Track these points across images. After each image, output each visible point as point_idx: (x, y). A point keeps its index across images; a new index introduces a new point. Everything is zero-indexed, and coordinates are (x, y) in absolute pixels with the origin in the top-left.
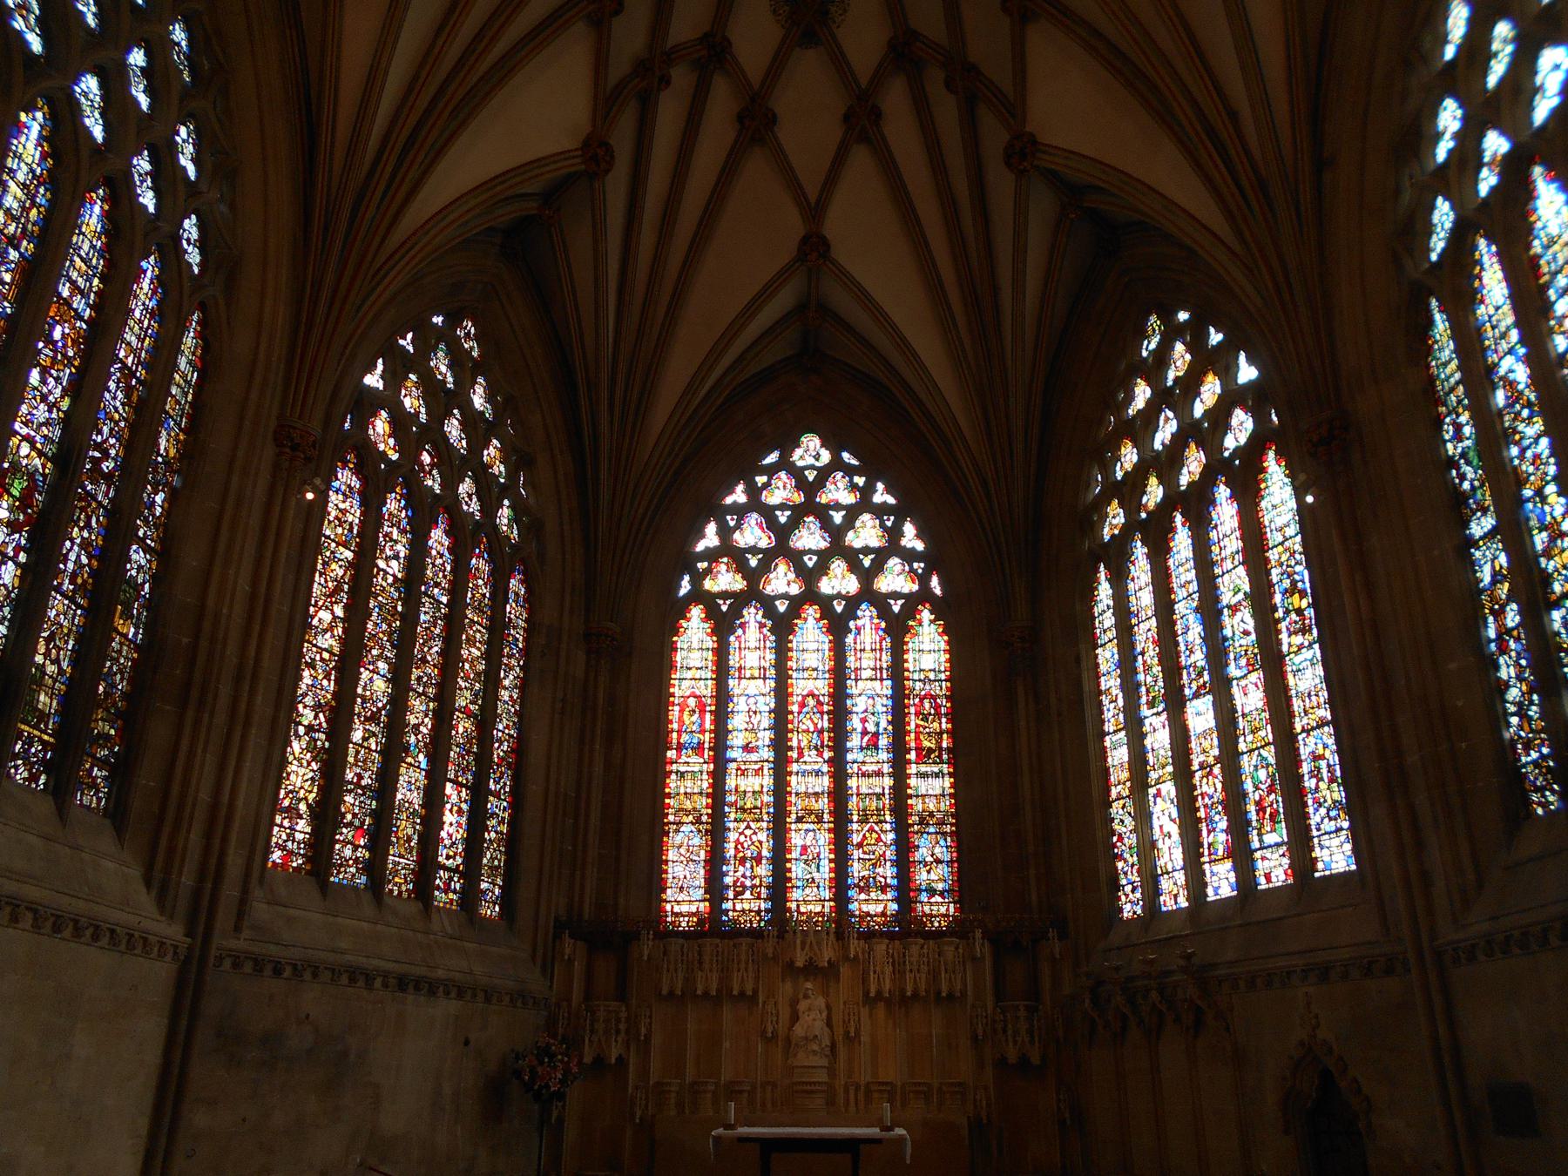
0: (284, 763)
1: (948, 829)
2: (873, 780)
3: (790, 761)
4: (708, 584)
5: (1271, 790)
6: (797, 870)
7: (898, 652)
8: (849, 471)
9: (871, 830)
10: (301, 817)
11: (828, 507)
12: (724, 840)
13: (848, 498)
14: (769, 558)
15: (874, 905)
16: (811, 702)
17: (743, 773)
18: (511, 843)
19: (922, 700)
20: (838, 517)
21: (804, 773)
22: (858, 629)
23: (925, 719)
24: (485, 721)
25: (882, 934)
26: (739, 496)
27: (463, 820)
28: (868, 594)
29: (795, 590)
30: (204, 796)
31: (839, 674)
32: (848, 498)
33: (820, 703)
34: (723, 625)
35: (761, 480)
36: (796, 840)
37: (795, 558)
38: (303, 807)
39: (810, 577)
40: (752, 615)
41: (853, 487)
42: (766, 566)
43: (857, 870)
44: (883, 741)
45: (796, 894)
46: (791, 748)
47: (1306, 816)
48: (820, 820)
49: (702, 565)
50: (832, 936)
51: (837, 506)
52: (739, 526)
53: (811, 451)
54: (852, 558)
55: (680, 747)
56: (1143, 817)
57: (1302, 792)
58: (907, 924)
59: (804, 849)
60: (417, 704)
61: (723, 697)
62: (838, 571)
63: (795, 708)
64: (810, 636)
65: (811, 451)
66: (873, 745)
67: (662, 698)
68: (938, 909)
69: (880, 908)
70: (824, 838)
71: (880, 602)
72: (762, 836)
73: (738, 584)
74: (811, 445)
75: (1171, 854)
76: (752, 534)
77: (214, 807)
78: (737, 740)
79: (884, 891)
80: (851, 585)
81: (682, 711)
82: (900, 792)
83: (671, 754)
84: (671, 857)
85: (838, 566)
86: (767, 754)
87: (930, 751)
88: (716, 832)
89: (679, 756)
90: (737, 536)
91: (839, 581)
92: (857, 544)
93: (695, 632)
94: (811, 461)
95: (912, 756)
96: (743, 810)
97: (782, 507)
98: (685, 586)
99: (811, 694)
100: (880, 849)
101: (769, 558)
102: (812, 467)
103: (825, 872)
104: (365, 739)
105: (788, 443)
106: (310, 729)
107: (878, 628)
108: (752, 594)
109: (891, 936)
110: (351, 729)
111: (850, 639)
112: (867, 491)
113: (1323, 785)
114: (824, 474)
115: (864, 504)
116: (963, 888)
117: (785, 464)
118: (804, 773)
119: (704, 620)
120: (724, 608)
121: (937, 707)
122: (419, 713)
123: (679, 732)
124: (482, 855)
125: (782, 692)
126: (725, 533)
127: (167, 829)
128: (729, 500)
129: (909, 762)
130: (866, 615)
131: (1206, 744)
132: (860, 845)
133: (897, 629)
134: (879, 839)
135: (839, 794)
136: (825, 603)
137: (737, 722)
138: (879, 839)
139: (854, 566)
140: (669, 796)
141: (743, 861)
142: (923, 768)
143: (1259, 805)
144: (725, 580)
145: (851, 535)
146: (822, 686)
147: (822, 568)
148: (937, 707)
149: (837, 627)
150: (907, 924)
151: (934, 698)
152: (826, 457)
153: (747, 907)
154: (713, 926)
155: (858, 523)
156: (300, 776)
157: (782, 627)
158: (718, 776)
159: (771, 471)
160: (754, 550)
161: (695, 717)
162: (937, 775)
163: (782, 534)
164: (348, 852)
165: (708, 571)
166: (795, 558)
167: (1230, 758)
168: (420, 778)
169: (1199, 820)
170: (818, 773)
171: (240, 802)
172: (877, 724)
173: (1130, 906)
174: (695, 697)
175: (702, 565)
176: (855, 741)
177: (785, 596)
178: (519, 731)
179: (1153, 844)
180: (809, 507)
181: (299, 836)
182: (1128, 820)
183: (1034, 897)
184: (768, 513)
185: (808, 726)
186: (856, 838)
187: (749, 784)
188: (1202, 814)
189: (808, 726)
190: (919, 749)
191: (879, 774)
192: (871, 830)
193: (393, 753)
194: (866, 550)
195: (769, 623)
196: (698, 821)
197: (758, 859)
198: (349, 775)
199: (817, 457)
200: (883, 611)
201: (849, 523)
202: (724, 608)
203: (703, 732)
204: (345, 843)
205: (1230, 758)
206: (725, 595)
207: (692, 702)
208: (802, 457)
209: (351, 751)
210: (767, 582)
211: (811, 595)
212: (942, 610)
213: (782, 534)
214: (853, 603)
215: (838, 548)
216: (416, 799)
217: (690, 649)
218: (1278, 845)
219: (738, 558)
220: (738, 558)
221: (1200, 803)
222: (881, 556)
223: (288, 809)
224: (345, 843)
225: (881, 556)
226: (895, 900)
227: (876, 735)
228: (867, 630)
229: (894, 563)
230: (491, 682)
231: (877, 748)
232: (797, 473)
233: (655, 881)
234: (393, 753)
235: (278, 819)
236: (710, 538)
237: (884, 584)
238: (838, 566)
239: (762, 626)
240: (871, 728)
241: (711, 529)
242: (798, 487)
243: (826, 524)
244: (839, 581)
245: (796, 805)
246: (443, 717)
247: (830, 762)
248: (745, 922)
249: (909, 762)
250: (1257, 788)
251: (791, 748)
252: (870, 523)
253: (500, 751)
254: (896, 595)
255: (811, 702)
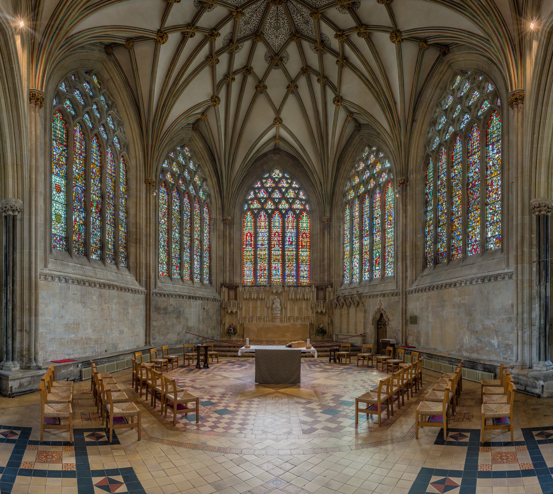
0: (159, 254)
1: (308, 263)
2: (291, 252)
3: (272, 248)
4: (251, 206)
5: (379, 258)
6: (274, 272)
7: (298, 223)
8: (287, 179)
9: (290, 263)
10: (164, 264)
11: (281, 188)
12: (257, 265)
13: (286, 185)
14: (266, 200)
15: (290, 280)
16: (277, 234)
17: (261, 250)
18: (210, 268)
19: (303, 234)
20: (284, 190)
21: (275, 250)
22: (288, 217)
23: (304, 238)
24: (201, 242)
25: (292, 286)
26: (259, 185)
27: (199, 263)
28: (290, 209)
29: (273, 207)
30: (144, 262)
31: (283, 228)
32: (286, 185)
33: (279, 234)
34: (256, 216)
35: (264, 181)
36: (273, 265)
37: (273, 200)
38: (164, 262)
39: (276, 204)
40: (262, 213)
41: (287, 183)
42: (266, 202)
43: (287, 272)
44: (294, 243)
45: (273, 277)
46: (272, 245)
47: (385, 264)
48: (279, 261)
49: (250, 202)
50: (281, 287)
51: (283, 187)
52: (259, 192)
53: (277, 174)
54: (287, 200)
55: (246, 245)
56: (351, 262)
57: (385, 259)
58: (298, 285)
59: (275, 267)
60: (186, 238)
61: (256, 233)
62: (284, 203)
63: (273, 235)
64: (277, 218)
65: (277, 174)
66: (291, 244)
67: (242, 234)
68: (305, 281)
69: (292, 281)
70: (280, 265)
71: (294, 211)
72: (266, 265)
73: (259, 206)
74: (277, 172)
75: (357, 270)
76: (262, 194)
77: (146, 264)
78: (260, 243)
79: (293, 277)
80: (287, 206)
81: (246, 237)
82: (297, 255)
83: (245, 246)
84: (245, 269)
85: (284, 202)
86: (266, 246)
87: (304, 246)
88: (255, 264)
89: (246, 247)
90: (259, 195)
91: (284, 205)
92: (288, 197)
93: (249, 217)
94: (277, 176)
95: (300, 247)
96: (261, 259)
97: (270, 187)
98: (246, 207)
99: (277, 232)
100: (292, 268)
101: (266, 200)
102: (277, 178)
103: (280, 273)
104: (175, 247)
105: (271, 171)
106: (163, 246)
107: (293, 217)
108: (263, 209)
109: (294, 287)
110: (172, 245)
111: (286, 219)
112: (291, 184)
113: (389, 258)
114: (280, 179)
115: (290, 187)
116: (310, 276)
117: (270, 177)
118: (275, 250)
119: (251, 215)
120: (256, 212)
121: (307, 236)
122: (186, 240)
123: (246, 241)
124: (204, 270)
125: (270, 232)
126: (255, 193)
127: (138, 269)
128: (256, 186)
129: (300, 248)
130: (290, 213)
131: (367, 247)
132: (288, 267)
133: (298, 217)
134: (292, 265)
135: (283, 255)
136: (280, 211)
137: (260, 238)
138: (292, 265)
139: (287, 202)
140: (244, 256)
141: (261, 270)
142: (303, 250)
143: (376, 261)
144: (256, 205)
145: (287, 194)
146: (279, 230)
147: (280, 202)
148: (307, 236)
149: (283, 216)
150: (298, 285)
151: (306, 234)
152: (281, 175)
153: (263, 280)
154: (255, 285)
155: (289, 191)
156: (163, 256)
157: (270, 217)
158: (255, 251)
159: (266, 178)
160: (263, 198)
161: (250, 238)
162: (306, 251)
163: (270, 194)
164: (175, 271)
165: (252, 203)
166: (273, 200)
167: (371, 250)
168: (188, 254)
169: (363, 264)
170: (278, 250)
171: (151, 262)
172: (292, 239)
173: (347, 281)
174: (250, 233)
175: (250, 202)
176: (287, 243)
177: (270, 209)
178: (209, 242)
179: (353, 268)
180: (277, 187)
181: (165, 269)
182: (348, 263)
183: (326, 279)
184: (266, 189)
185: (276, 240)
186: (287, 265)
187: (263, 253)
188: (364, 262)
189: (276, 240)
190: (302, 245)
191: (292, 251)
192: (290, 263)
193: (182, 249)
194: (291, 198)
195: (267, 216)
196: (251, 261)
197: (265, 270)
198: (173, 255)
199: (278, 175)
200: (294, 213)
201: (287, 191)
202: (256, 212)
203: (251, 241)
204: (174, 269)
205: (371, 250)
206: (256, 209)
207: (249, 234)
208: (274, 175)
209: (173, 250)
210: (266, 206)
211: (277, 209)
212: (308, 213)
213: (270, 194)
214: (287, 211)
215: (284, 197)
216: (188, 259)
217: (248, 222)
218: (379, 269)
219: (259, 200)
220: (259, 200)
221: (364, 260)
222: (294, 199)
223: (162, 263)
224: (174, 269)
225: (294, 199)
226: (296, 279)
227: (292, 242)
228: (290, 217)
229: (298, 201)
230: (202, 231)
231: (292, 244)
232: (273, 179)
233: (242, 275)
234: (182, 249)
235: (160, 265)
236: (252, 195)
237: (295, 206)
238: (284, 202)
239: (265, 216)
240: (291, 240)
241: (252, 193)
242: (273, 183)
243: (280, 191)
244: (284, 205)
245: (273, 258)
246: (192, 240)
247: (281, 248)
248: (262, 283)
249: (300, 248)
250: (376, 257)
251: (272, 245)
252: (291, 192)
253: (206, 247)
254: (298, 209)
255: (277, 234)
